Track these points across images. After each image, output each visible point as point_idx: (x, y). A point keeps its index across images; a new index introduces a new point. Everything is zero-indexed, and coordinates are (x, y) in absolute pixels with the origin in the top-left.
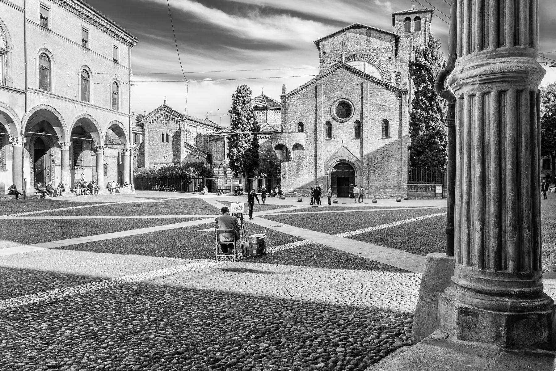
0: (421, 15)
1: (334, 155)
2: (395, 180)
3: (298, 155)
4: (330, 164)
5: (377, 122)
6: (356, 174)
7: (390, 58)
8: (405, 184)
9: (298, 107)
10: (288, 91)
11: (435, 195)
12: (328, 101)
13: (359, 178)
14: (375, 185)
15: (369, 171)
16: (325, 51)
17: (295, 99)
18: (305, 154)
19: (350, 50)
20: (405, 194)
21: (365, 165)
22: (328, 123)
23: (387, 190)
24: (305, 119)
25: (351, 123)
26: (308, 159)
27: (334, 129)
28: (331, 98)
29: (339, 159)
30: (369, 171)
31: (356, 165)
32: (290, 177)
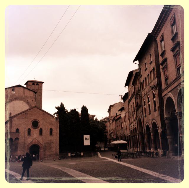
0: (39, 84)
1: (31, 142)
2: (55, 151)
3: (16, 142)
4: (30, 146)
6: (40, 150)
7: (33, 101)
8: (58, 153)
9: (17, 122)
10: (12, 115)
11: (69, 157)
12: (30, 120)
13: (41, 152)
14: (48, 154)
15: (45, 148)
17: (15, 119)
18: (19, 142)
19: (16, 96)
20: (58, 157)
21: (44, 146)
23: (52, 156)
25: (39, 129)
27: (32, 131)
28: (31, 119)
29: (33, 144)
30: (45, 148)
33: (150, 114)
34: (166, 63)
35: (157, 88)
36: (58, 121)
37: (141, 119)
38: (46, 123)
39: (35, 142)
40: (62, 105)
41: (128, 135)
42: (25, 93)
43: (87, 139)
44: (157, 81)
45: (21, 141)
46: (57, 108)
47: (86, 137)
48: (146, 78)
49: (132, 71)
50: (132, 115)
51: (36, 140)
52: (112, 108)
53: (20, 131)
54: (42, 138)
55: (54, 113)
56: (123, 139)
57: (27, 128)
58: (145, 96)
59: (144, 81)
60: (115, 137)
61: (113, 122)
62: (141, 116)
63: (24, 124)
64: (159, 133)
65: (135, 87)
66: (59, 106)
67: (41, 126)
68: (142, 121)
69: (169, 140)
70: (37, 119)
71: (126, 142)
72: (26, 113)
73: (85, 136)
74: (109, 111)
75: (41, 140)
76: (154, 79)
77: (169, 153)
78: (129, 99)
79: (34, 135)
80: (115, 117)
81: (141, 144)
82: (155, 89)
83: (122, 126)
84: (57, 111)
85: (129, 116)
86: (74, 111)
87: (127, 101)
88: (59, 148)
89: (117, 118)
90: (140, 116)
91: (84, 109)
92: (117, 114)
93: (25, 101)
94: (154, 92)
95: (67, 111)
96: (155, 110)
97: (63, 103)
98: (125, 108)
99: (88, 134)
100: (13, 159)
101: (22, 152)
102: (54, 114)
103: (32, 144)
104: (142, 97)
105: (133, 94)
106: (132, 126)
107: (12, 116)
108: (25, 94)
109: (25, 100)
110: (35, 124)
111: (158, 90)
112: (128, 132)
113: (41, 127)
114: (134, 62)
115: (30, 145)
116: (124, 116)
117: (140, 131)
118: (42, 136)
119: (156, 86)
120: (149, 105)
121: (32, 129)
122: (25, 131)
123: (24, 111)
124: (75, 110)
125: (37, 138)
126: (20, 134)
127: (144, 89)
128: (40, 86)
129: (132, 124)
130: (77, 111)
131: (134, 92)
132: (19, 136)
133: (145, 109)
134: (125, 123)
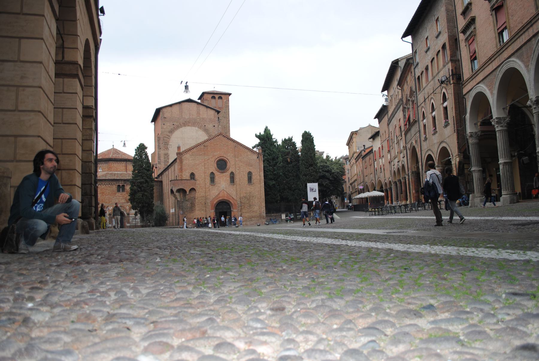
0: (222, 96)
4: (215, 203)
5: (244, 173)
6: (232, 209)
7: (214, 126)
8: (264, 214)
13: (235, 212)
16: (165, 116)
17: (187, 156)
18: (196, 196)
20: (264, 220)
21: (239, 202)
22: (212, 173)
23: (253, 219)
24: (196, 170)
25: (228, 174)
26: (198, 199)
29: (221, 199)
31: (233, 202)
32: (186, 213)
33: (434, 134)
34: (472, 27)
35: (452, 82)
36: (260, 159)
37: (416, 147)
38: (241, 162)
39: (223, 196)
40: (267, 130)
41: (387, 181)
42: (201, 113)
43: (313, 190)
44: (451, 69)
45: (199, 194)
46: (259, 137)
47: (312, 187)
48: (427, 66)
49: (398, 59)
50: (396, 142)
51: (225, 192)
52: (354, 136)
53: (197, 177)
55: (254, 145)
56: (376, 189)
58: (425, 101)
59: (424, 72)
60: (361, 187)
61: (356, 162)
62: (416, 141)
63: (203, 164)
64: (454, 166)
65: (402, 90)
66: (262, 133)
67: (231, 167)
68: (418, 150)
69: (474, 174)
70: (225, 156)
71: (382, 194)
72: (204, 146)
73: (309, 185)
74: (349, 143)
75: (234, 193)
76: (444, 66)
77: (474, 197)
78: (389, 116)
80: (361, 152)
81: (414, 191)
82: (447, 84)
83: (376, 167)
84: (257, 141)
85: (389, 147)
86: (289, 142)
87: (386, 119)
88: (264, 205)
89: (365, 153)
90: (414, 142)
91: (307, 138)
92: (364, 146)
93: (200, 128)
94: (444, 90)
95: (276, 141)
96: (446, 126)
97: (269, 128)
98: (381, 133)
99: (314, 182)
100: (189, 224)
101: (202, 212)
102: (253, 148)
103: (218, 200)
104: (419, 104)
105: (399, 103)
106: (396, 164)
107: (181, 151)
108: (200, 114)
109: (200, 125)
110: (222, 165)
111: (452, 85)
112: (388, 175)
114: (404, 39)
115: (216, 201)
116: (379, 148)
117: (412, 170)
118: (235, 186)
119: (450, 77)
120: (434, 118)
121: (217, 174)
122: (206, 177)
123: (201, 143)
124: (290, 140)
125: (226, 188)
126: (198, 182)
127: (424, 89)
128: (225, 101)
129: (396, 160)
130: (293, 141)
131: (401, 100)
132: (197, 185)
133: (425, 126)
134: (380, 160)
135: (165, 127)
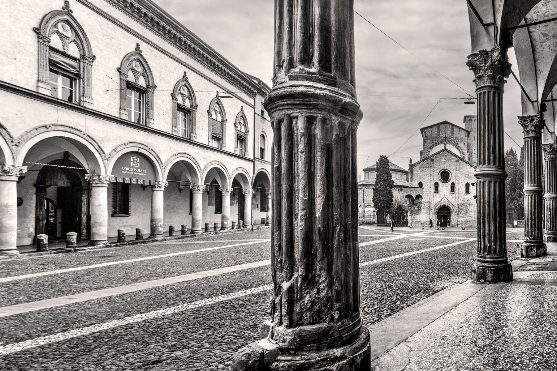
10: (413, 163)
24: (423, 180)
28: (438, 169)
29: (442, 204)
31: (452, 208)
39: (444, 202)
51: (446, 199)
53: (423, 186)
54: (454, 197)
57: (433, 183)
70: (448, 169)
72: (432, 160)
75: (454, 200)
79: (443, 191)
110: (445, 176)
113: (452, 179)
115: (438, 206)
121: (440, 184)
135: (426, 144)
